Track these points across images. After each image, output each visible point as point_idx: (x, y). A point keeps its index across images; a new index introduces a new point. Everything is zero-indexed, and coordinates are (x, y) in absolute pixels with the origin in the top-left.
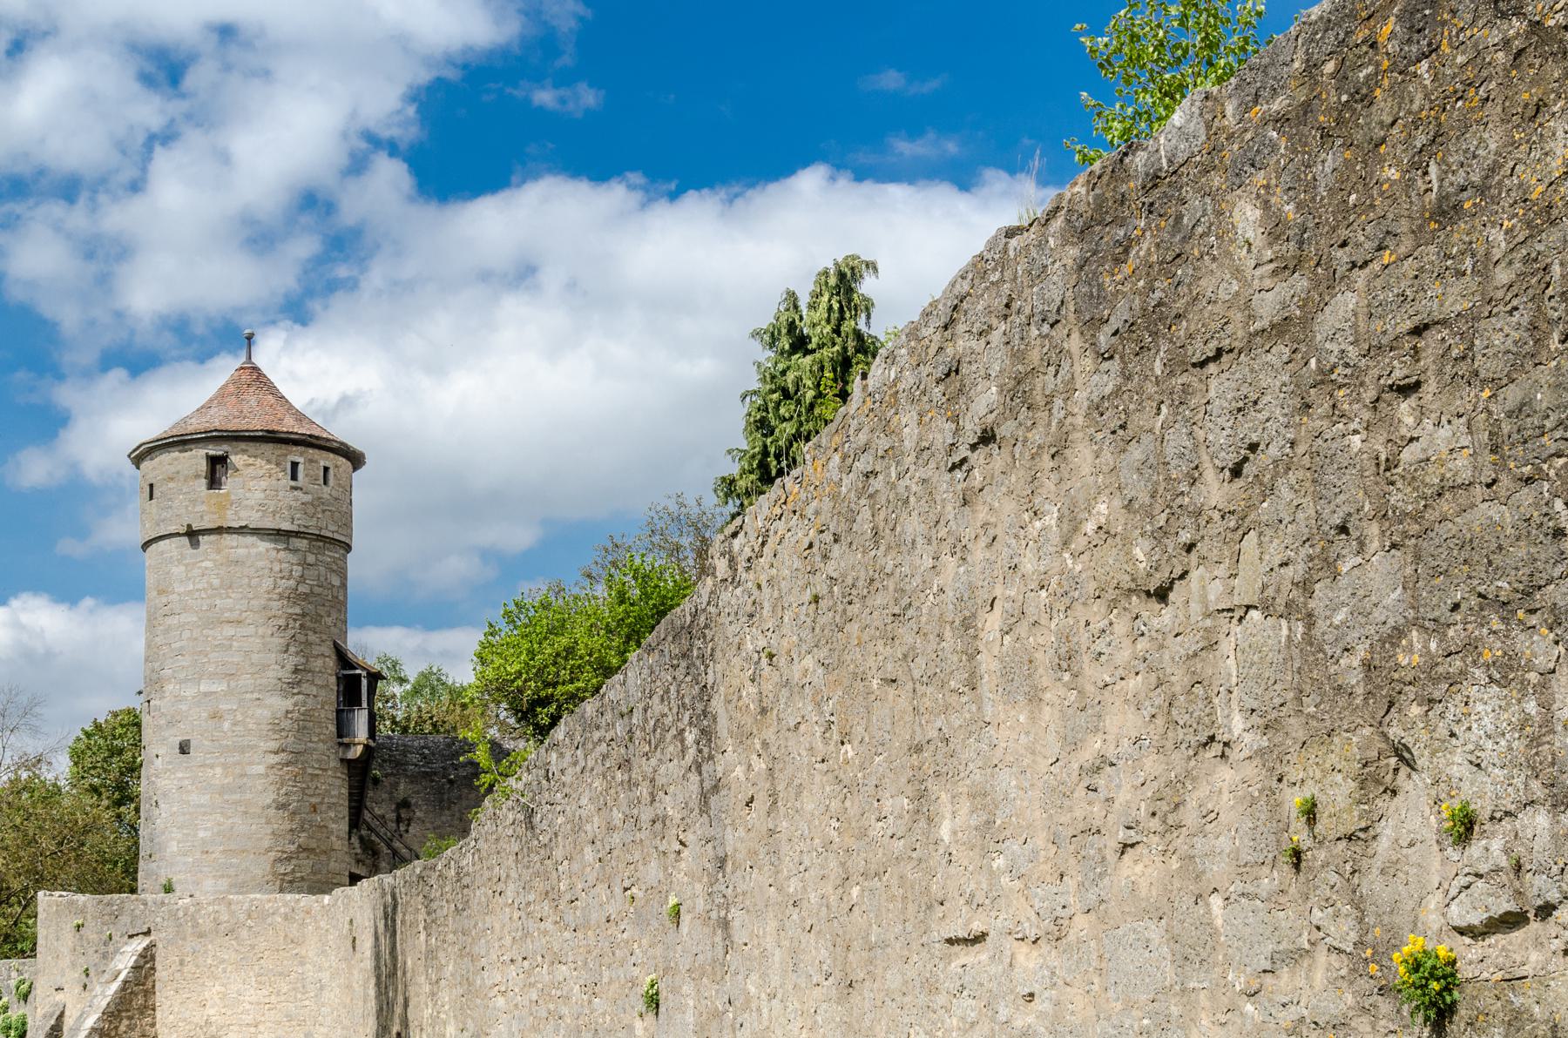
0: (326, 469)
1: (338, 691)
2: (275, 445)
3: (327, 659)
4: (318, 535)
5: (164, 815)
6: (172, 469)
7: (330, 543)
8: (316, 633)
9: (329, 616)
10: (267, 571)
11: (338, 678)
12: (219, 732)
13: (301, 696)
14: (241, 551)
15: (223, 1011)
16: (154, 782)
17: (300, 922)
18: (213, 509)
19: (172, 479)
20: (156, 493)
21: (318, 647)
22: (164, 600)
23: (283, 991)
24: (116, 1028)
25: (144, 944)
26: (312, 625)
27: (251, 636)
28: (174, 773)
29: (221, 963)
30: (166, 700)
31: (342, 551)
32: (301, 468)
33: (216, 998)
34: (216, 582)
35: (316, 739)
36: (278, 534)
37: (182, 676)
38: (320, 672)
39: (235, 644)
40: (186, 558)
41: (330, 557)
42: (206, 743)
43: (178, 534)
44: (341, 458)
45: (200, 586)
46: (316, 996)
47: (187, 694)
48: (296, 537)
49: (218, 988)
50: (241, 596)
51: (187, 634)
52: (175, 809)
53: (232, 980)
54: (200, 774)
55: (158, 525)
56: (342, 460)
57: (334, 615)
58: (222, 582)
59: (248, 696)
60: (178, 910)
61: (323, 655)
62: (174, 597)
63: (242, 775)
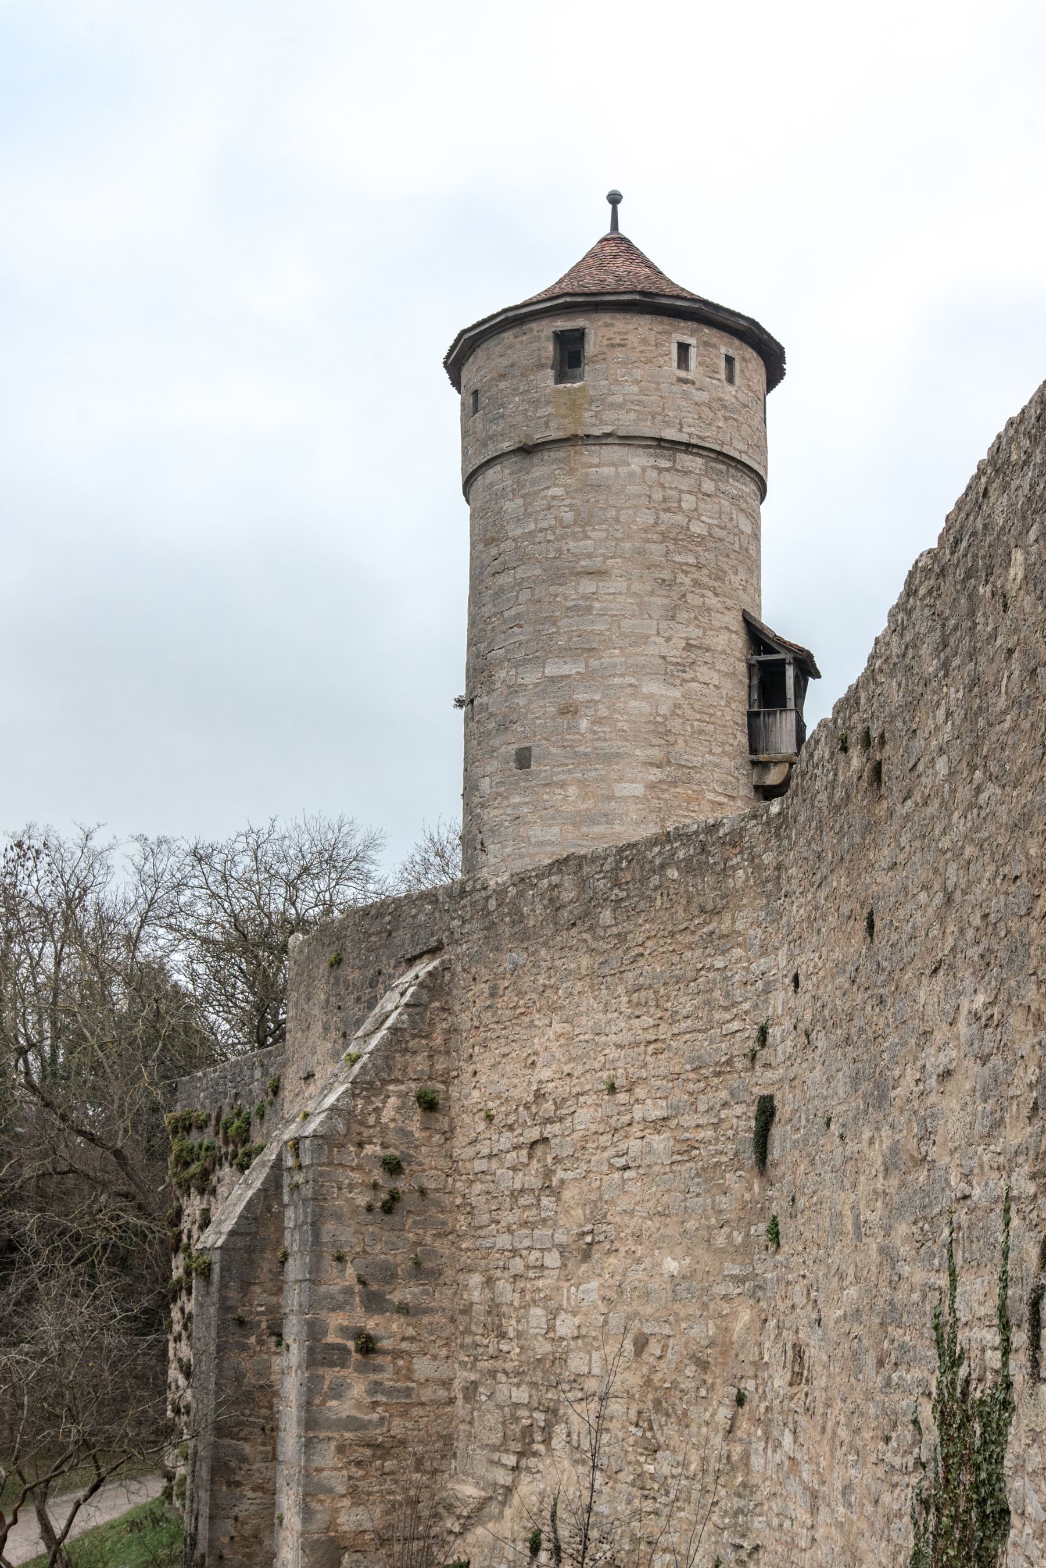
0: (730, 360)
1: (750, 687)
2: (654, 317)
3: (734, 636)
4: (719, 453)
5: (492, 860)
6: (504, 362)
7: (736, 467)
8: (716, 595)
9: (736, 573)
10: (644, 501)
11: (750, 667)
12: (574, 734)
13: (695, 684)
14: (605, 470)
15: (567, 1069)
16: (478, 816)
17: (718, 868)
18: (563, 411)
19: (503, 376)
20: (483, 401)
21: (719, 616)
22: (494, 552)
23: (685, 1012)
24: (377, 1110)
25: (430, 968)
26: (712, 583)
27: (620, 593)
28: (507, 798)
29: (562, 980)
30: (495, 694)
31: (753, 487)
32: (693, 352)
33: (554, 1046)
34: (568, 516)
35: (719, 750)
36: (660, 447)
37: (519, 655)
38: (724, 652)
39: (596, 605)
40: (523, 487)
41: (736, 488)
42: (553, 750)
43: (513, 452)
44: (750, 350)
45: (545, 524)
46: (756, 1006)
47: (527, 681)
48: (686, 452)
49: (557, 1027)
50: (604, 535)
51: (525, 595)
52: (509, 850)
53: (583, 1009)
54: (546, 797)
55: (485, 445)
56: (750, 353)
57: (742, 575)
58: (578, 513)
59: (616, 680)
60: (489, 897)
61: (727, 628)
62: (509, 545)
63: (610, 798)
